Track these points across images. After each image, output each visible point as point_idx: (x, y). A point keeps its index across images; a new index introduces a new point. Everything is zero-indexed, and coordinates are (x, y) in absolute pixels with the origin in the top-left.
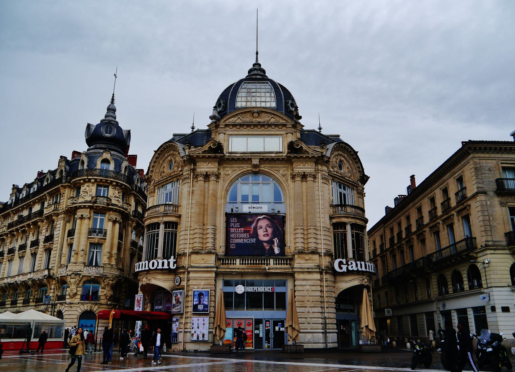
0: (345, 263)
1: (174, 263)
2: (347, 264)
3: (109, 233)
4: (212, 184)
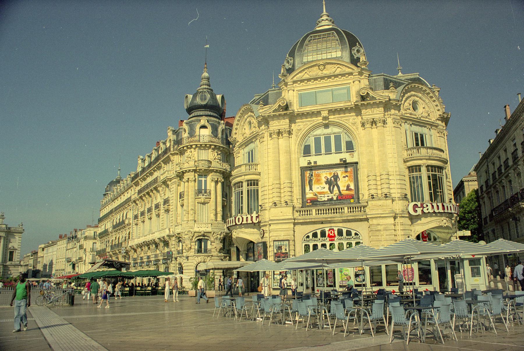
0: (419, 206)
1: (257, 217)
2: (422, 206)
3: (213, 192)
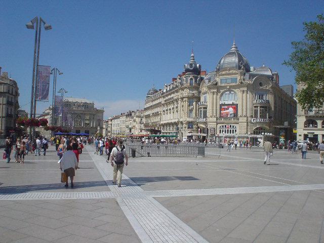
4: (215, 96)
